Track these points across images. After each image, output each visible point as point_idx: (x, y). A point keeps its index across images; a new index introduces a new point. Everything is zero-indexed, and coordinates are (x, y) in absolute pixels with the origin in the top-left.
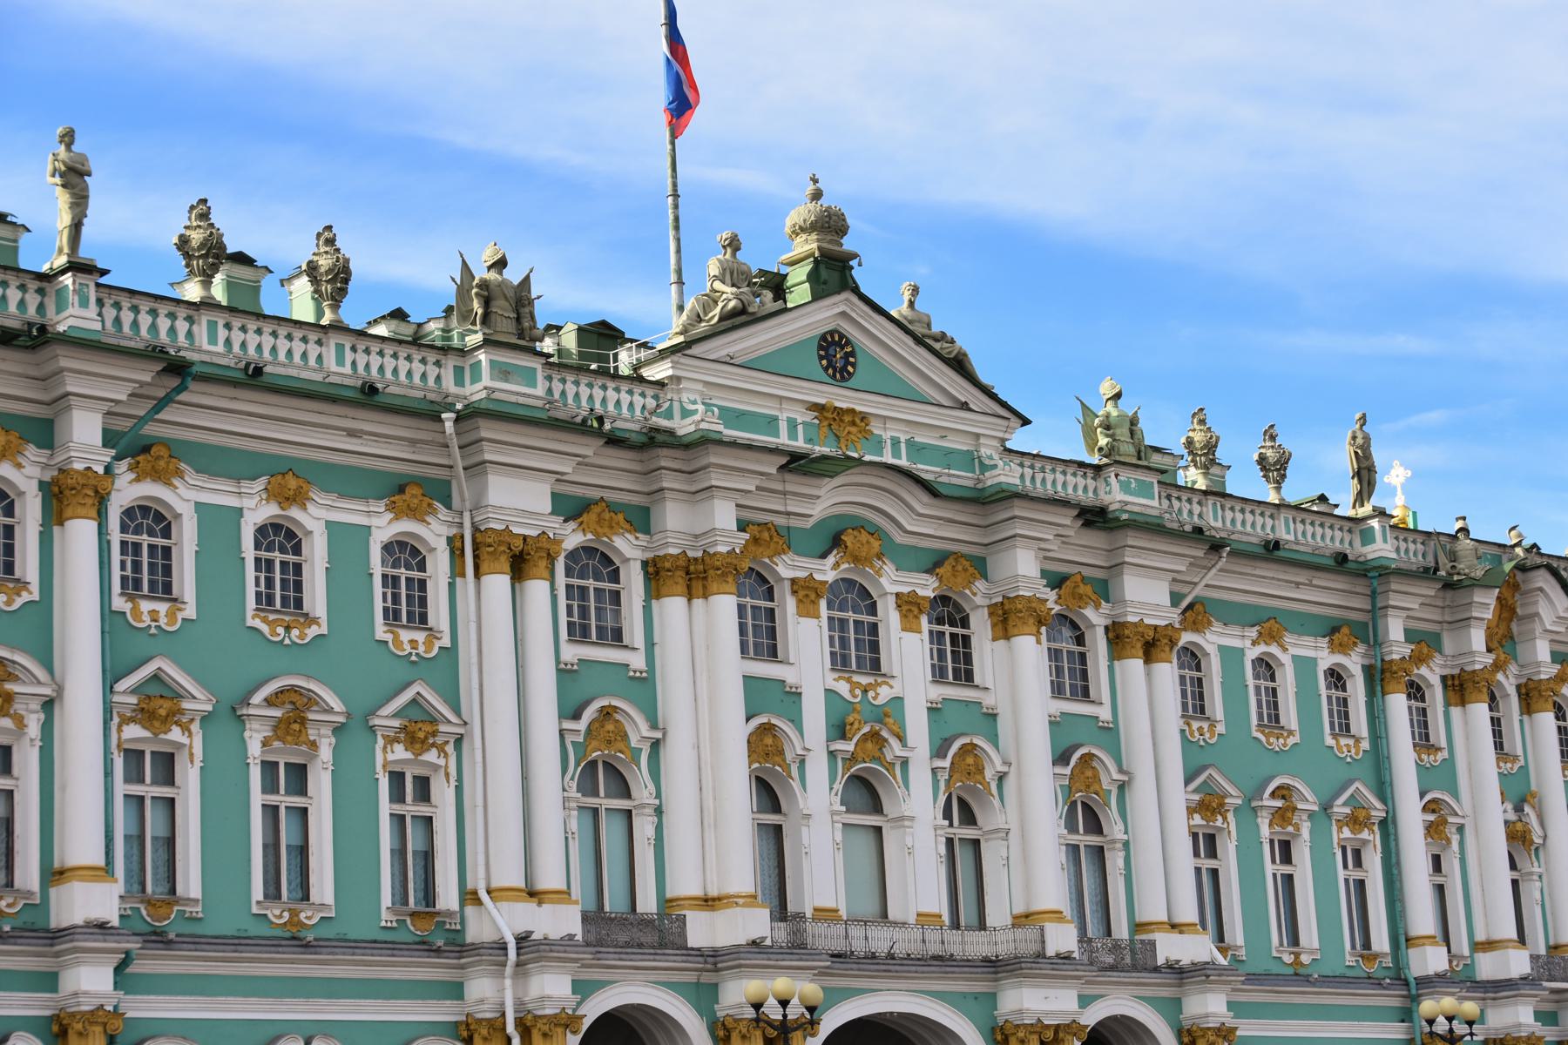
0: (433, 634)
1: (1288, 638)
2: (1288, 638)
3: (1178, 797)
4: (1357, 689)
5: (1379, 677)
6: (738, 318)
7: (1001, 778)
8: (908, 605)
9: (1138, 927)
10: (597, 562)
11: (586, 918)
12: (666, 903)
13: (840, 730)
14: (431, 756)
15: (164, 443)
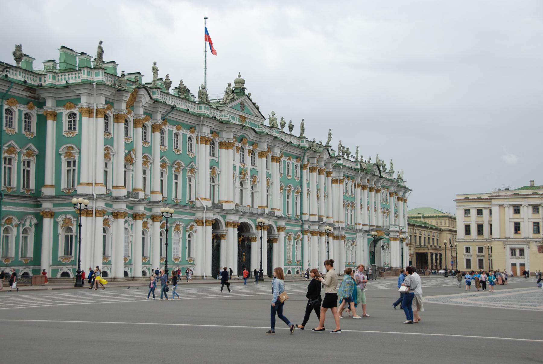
0: (194, 153)
1: (292, 159)
2: (292, 159)
3: (279, 187)
4: (299, 168)
5: (303, 167)
6: (233, 100)
7: (258, 182)
8: (249, 151)
9: (272, 209)
10: (212, 143)
11: (213, 204)
12: (219, 201)
13: (241, 173)
14: (193, 175)
15: (167, 119)
